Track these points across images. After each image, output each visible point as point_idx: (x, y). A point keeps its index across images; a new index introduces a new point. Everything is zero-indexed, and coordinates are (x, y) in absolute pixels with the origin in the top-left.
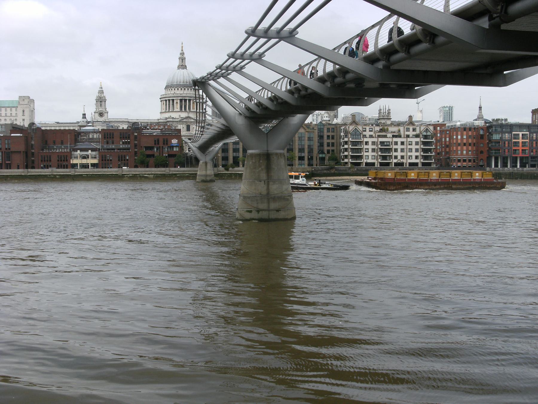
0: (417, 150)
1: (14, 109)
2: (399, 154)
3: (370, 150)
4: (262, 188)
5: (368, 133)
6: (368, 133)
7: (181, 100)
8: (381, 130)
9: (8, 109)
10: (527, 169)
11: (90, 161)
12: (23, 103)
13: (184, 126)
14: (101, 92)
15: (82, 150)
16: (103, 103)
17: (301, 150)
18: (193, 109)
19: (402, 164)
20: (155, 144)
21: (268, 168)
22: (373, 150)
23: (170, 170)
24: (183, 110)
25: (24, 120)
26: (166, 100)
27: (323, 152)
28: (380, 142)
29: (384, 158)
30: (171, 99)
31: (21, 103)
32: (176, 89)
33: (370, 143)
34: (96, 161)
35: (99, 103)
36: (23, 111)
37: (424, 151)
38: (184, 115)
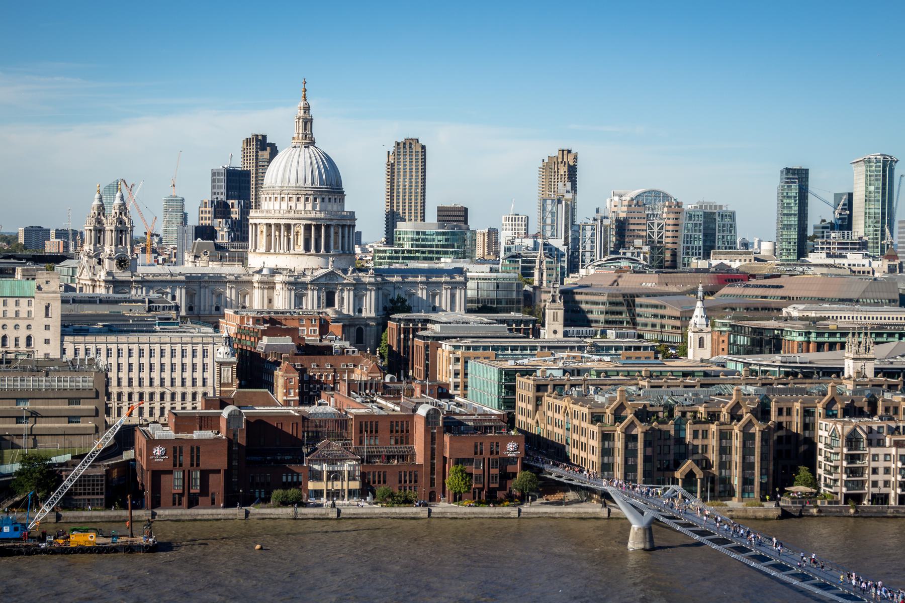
3: (881, 471)
7: (308, 228)
15: (332, 462)
20: (476, 453)
23: (520, 511)
24: (313, 251)
28: (901, 456)
30: (282, 222)
33: (881, 457)
34: (355, 485)
36: (47, 308)
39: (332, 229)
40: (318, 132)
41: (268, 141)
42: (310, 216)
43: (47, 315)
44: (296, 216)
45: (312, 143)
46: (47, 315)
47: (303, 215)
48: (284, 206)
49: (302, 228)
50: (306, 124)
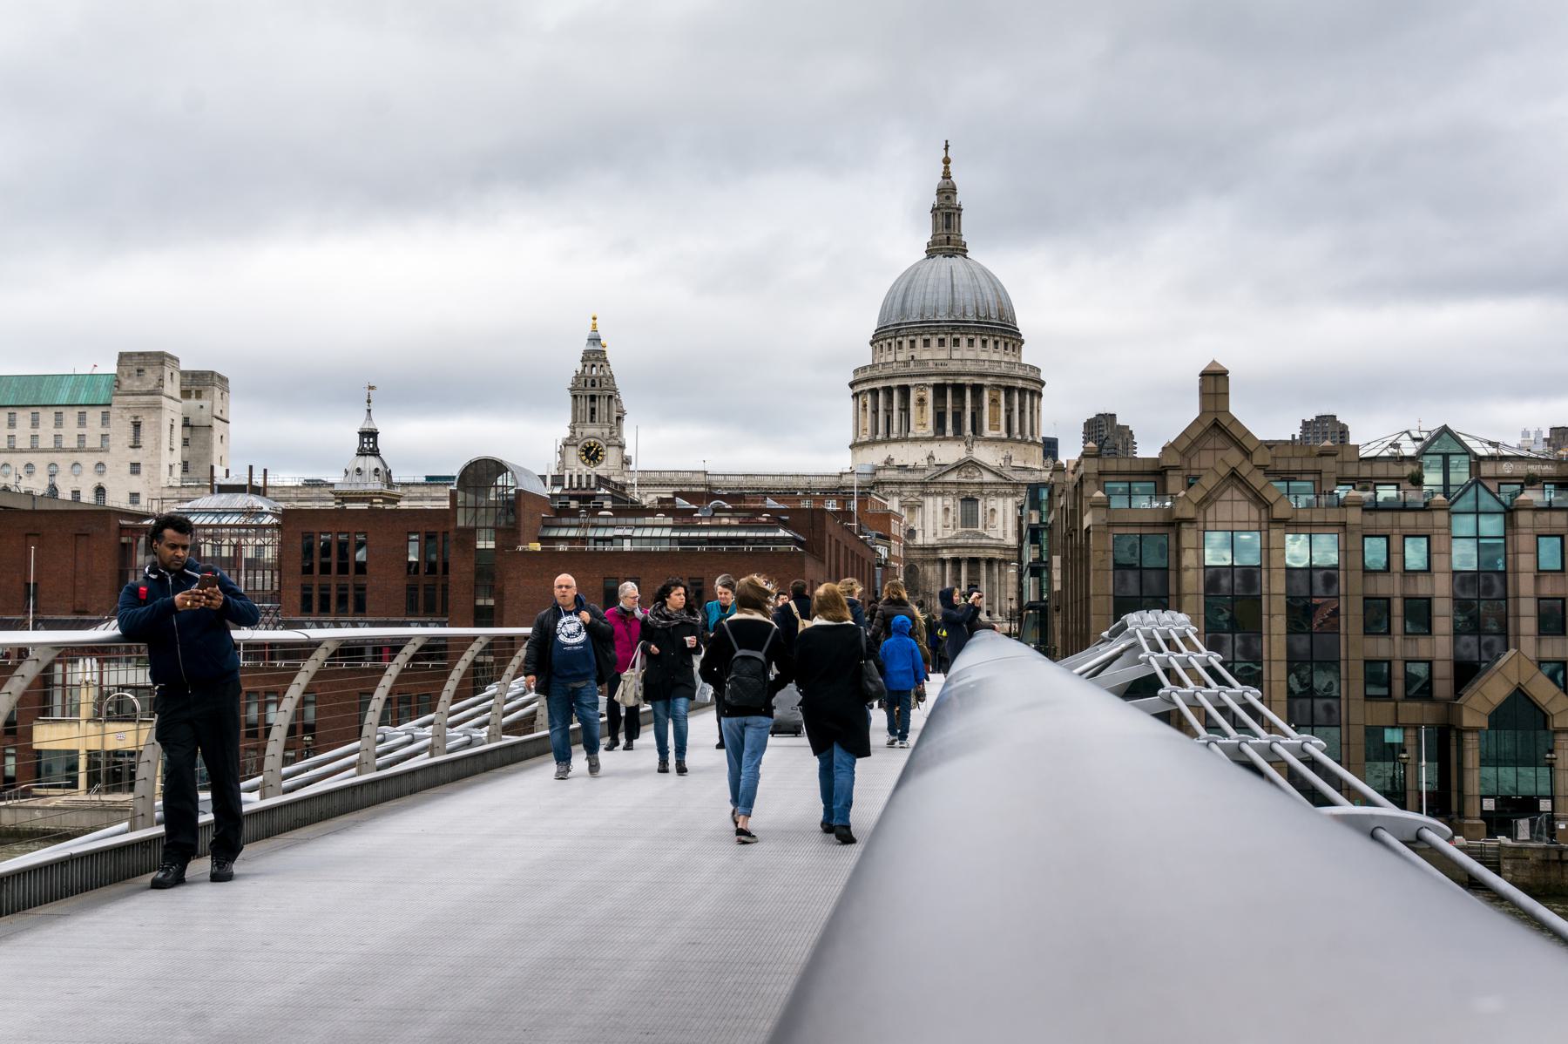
1: (94, 416)
7: (939, 390)
9: (71, 416)
12: (136, 385)
13: (949, 502)
14: (595, 355)
16: (601, 406)
18: (994, 426)
24: (949, 433)
25: (135, 468)
26: (875, 392)
30: (895, 383)
31: (127, 384)
32: (919, 343)
35: (585, 405)
36: (137, 426)
38: (950, 453)
39: (986, 394)
40: (968, 229)
41: (1120, 421)
42: (942, 369)
43: (136, 445)
44: (918, 370)
45: (959, 250)
46: (136, 445)
47: (931, 367)
48: (901, 357)
49: (930, 392)
50: (948, 216)
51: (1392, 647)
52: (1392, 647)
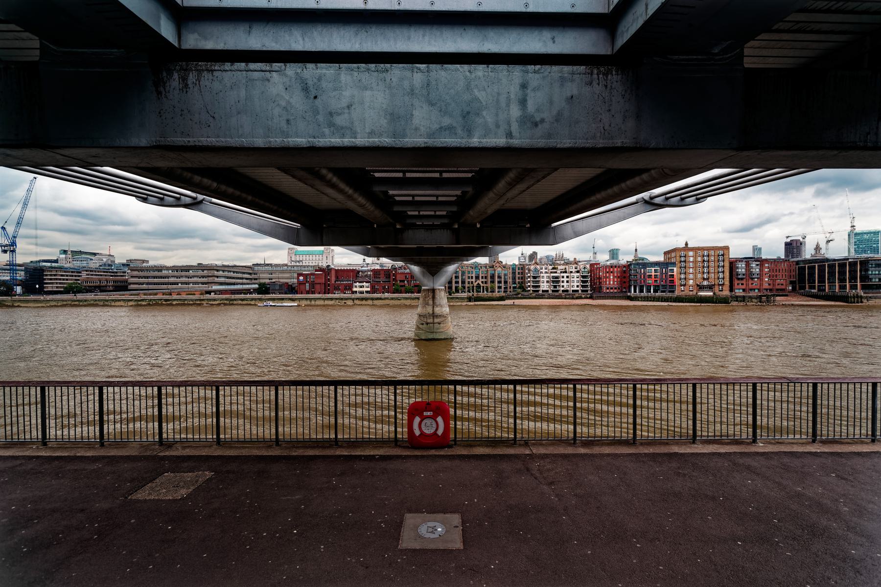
0: (578, 282)
2: (565, 284)
4: (429, 309)
5: (544, 271)
6: (544, 271)
8: (553, 268)
10: (658, 294)
11: (365, 289)
15: (360, 282)
17: (500, 282)
19: (567, 291)
21: (434, 298)
22: (548, 282)
27: (515, 283)
29: (555, 287)
34: (369, 289)
37: (583, 282)
51: (470, 280)
52: (470, 280)
